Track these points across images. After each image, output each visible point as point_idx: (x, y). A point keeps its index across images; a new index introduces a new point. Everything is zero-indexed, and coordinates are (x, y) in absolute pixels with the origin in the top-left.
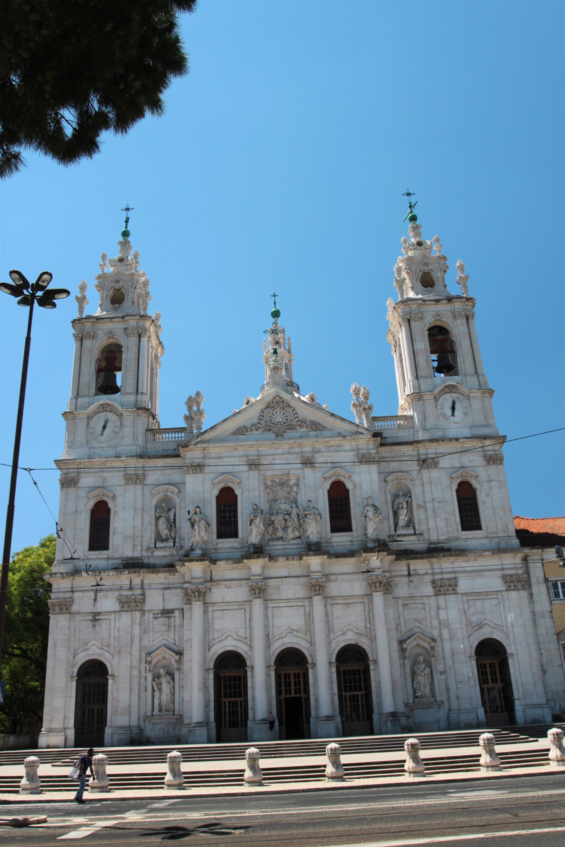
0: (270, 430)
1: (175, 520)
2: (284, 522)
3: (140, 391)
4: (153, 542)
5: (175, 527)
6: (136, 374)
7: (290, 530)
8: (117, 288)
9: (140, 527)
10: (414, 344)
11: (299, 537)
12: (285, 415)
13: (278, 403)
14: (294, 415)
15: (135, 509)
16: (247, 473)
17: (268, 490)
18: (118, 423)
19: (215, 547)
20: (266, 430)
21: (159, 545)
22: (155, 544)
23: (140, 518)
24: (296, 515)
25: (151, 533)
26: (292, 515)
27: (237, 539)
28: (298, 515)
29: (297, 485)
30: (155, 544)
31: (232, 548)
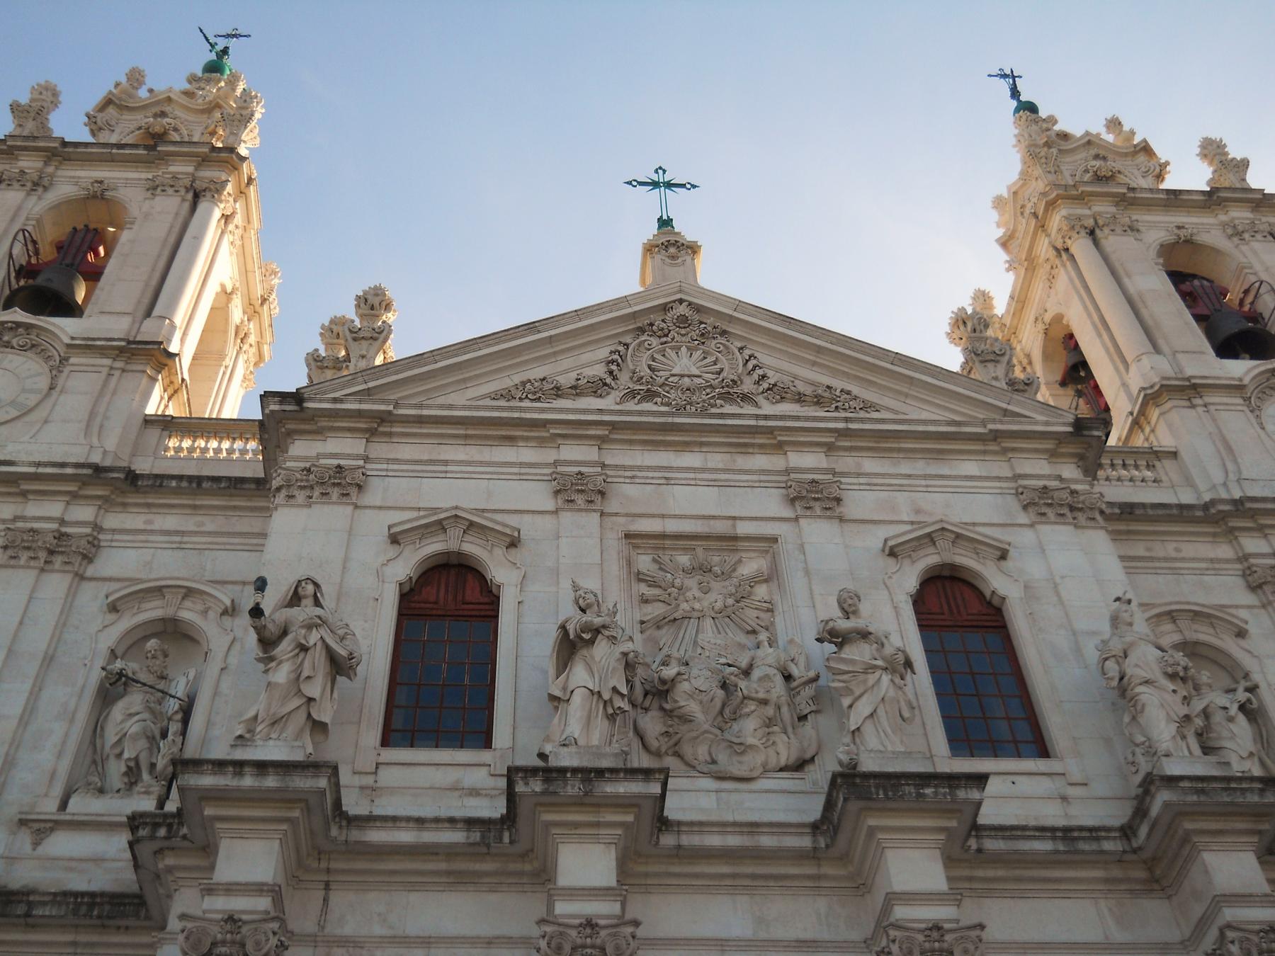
0: (650, 395)
1: (186, 712)
2: (720, 693)
3: (156, 312)
4: (58, 791)
5: (184, 733)
6: (157, 275)
7: (749, 729)
8: (158, 129)
9: (14, 722)
10: (1126, 281)
11: (800, 765)
12: (710, 359)
13: (683, 321)
14: (747, 361)
15: (10, 650)
16: (547, 522)
17: (643, 588)
18: (44, 383)
19: (369, 780)
20: (632, 394)
21: (81, 805)
22: (63, 805)
23: (27, 686)
24: (779, 679)
25: (60, 755)
26: (756, 674)
27: (485, 756)
28: (788, 678)
29: (771, 576)
30: (63, 805)
31: (454, 788)
